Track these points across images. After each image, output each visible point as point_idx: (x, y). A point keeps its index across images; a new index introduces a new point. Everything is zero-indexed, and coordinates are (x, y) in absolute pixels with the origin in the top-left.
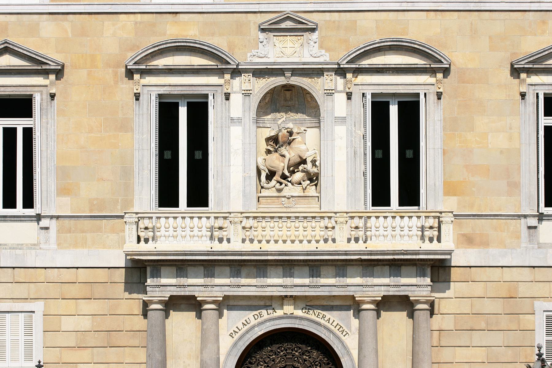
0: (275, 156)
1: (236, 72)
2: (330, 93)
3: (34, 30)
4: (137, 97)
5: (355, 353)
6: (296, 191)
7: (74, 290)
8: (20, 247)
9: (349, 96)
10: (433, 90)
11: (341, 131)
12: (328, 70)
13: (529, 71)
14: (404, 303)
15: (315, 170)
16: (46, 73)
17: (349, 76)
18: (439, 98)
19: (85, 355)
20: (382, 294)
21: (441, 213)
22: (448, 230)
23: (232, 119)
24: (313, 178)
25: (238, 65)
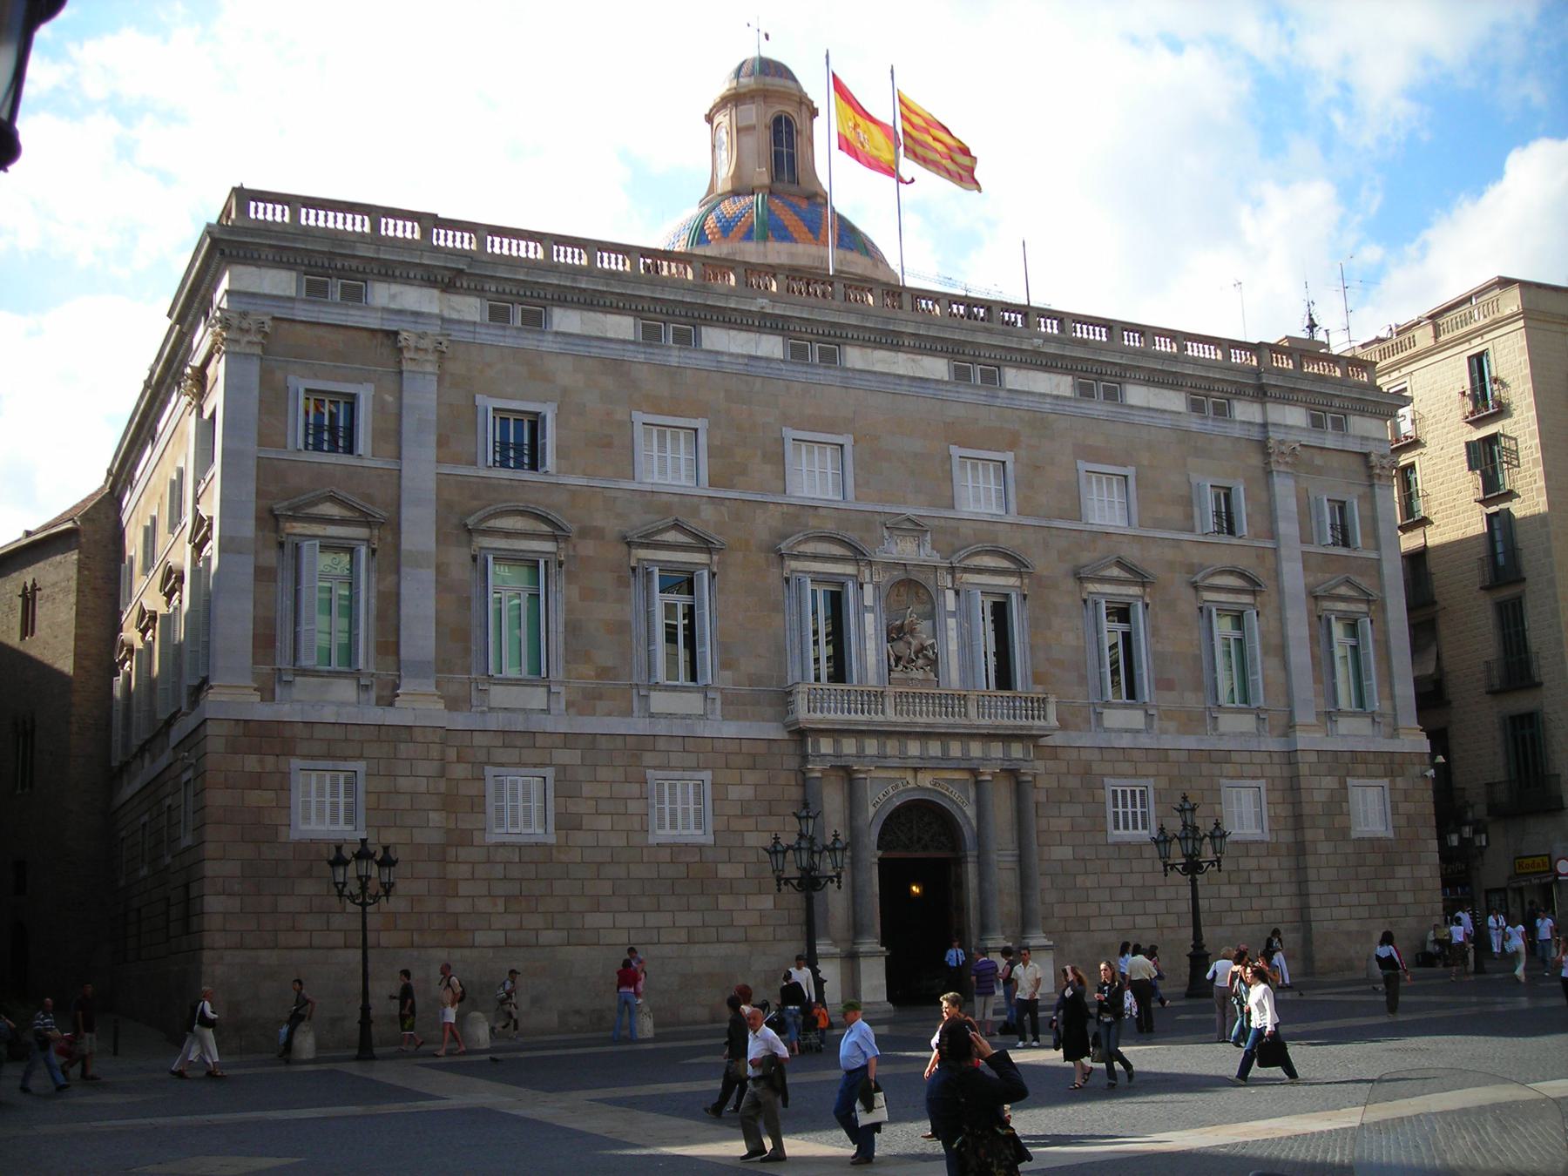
0: (901, 644)
1: (870, 563)
2: (941, 591)
3: (695, 511)
5: (974, 823)
6: (919, 675)
8: (688, 716)
9: (957, 593)
14: (1013, 774)
22: (1052, 710)
24: (933, 663)
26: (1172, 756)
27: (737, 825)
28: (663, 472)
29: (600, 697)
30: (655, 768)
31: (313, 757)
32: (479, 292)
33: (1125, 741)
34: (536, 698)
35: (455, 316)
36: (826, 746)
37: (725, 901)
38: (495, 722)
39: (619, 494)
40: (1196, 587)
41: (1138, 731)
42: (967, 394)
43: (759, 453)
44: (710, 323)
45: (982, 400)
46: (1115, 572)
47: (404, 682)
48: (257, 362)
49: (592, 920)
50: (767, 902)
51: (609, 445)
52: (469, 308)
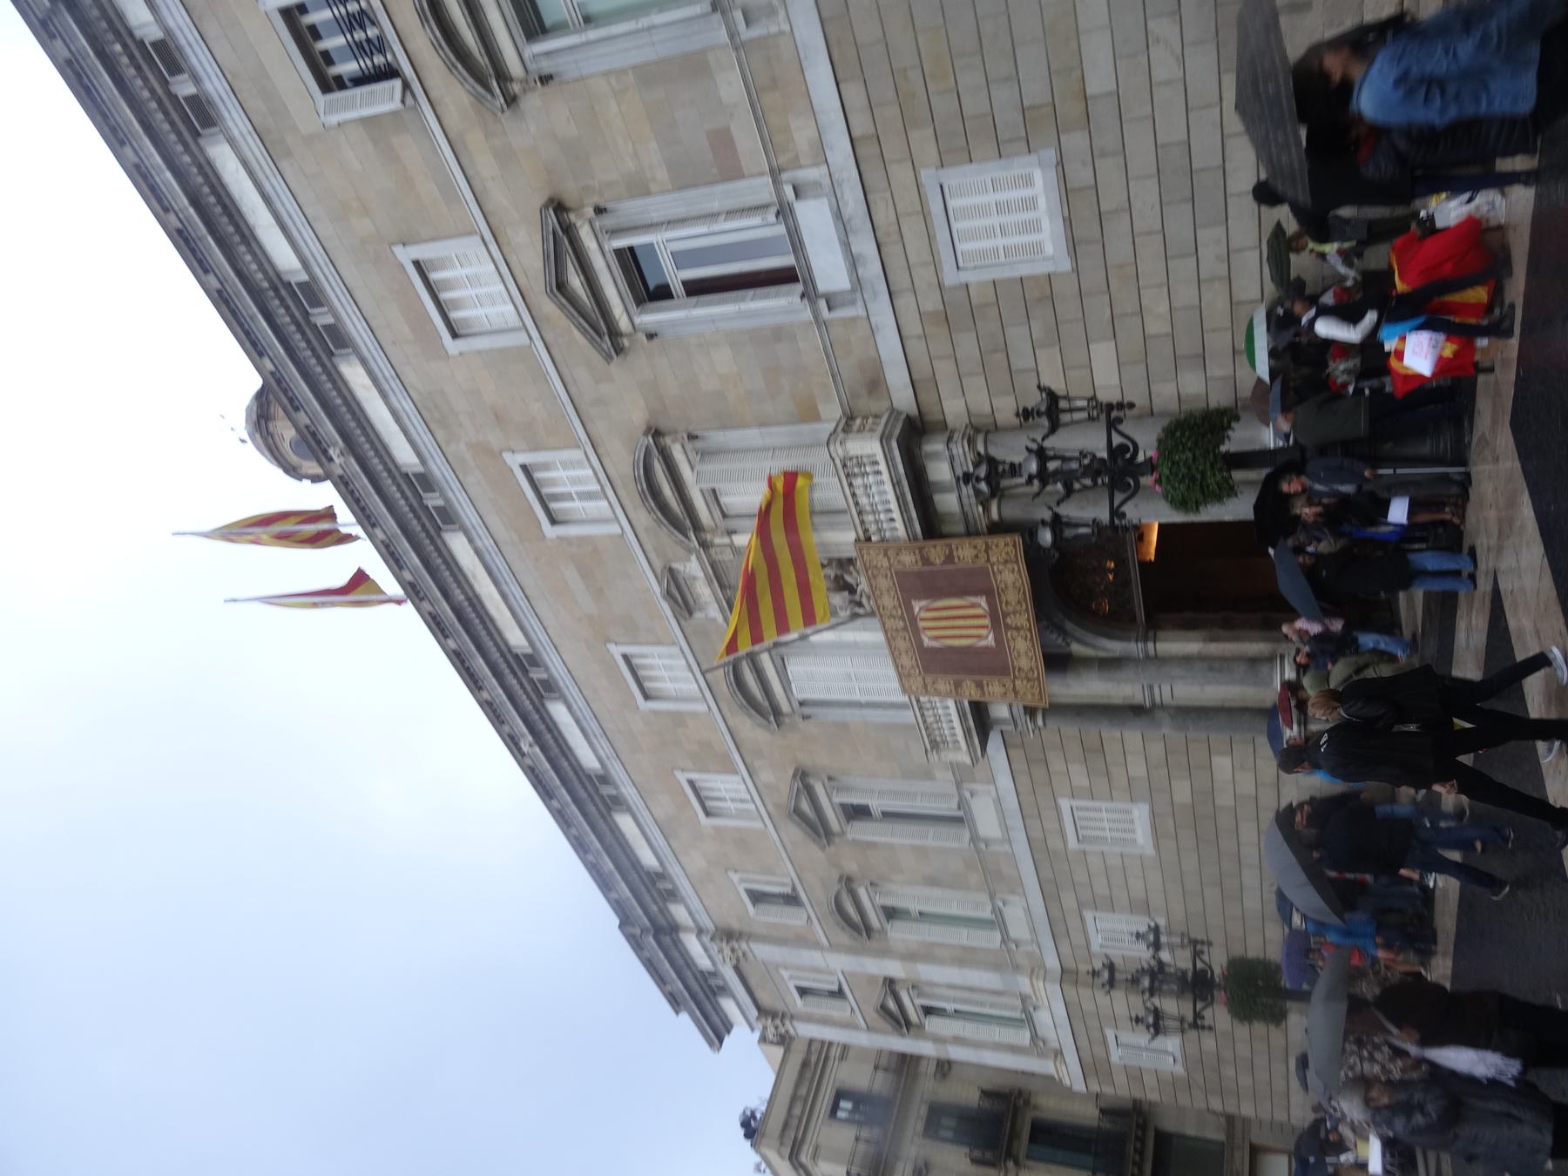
4: (805, 717)
9: (730, 533)
12: (709, 557)
13: (614, 333)
16: (809, 791)
17: (709, 537)
26: (861, 125)
30: (1065, 842)
32: (664, 912)
33: (865, 246)
34: (1015, 915)
37: (1225, 799)
39: (785, 840)
40: (511, 100)
41: (838, 215)
44: (577, 767)
45: (462, 497)
46: (575, 282)
48: (796, 1023)
50: (1222, 764)
52: (679, 912)
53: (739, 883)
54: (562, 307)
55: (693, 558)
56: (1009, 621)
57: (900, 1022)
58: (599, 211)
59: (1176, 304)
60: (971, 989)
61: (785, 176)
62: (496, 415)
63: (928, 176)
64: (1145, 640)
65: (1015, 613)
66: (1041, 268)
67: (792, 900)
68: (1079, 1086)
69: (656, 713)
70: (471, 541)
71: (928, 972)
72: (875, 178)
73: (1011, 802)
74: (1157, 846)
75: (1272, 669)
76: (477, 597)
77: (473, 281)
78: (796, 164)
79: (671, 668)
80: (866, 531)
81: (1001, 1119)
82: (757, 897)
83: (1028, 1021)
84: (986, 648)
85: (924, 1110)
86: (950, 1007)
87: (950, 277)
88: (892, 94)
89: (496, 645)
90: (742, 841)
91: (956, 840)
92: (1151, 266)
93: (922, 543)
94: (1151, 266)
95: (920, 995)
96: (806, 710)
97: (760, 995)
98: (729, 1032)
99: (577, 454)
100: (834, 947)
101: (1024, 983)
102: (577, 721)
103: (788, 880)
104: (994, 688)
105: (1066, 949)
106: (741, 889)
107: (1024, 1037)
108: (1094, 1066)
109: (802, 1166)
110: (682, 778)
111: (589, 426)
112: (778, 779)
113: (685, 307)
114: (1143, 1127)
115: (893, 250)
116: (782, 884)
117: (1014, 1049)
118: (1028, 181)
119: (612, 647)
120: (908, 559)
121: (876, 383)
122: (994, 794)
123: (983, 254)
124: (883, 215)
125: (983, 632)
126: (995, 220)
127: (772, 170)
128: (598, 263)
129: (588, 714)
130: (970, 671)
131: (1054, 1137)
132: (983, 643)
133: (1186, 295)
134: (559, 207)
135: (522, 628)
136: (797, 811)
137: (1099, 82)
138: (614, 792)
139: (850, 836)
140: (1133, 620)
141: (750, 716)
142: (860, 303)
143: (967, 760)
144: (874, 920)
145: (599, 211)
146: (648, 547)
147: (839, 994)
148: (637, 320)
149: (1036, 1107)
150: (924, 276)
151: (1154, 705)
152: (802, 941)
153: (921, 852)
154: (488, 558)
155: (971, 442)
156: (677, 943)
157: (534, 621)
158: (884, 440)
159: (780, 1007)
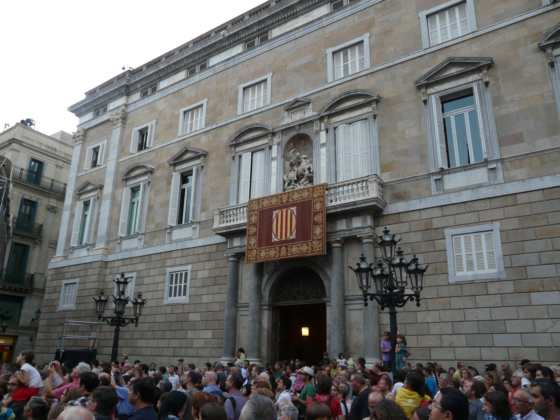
1: (274, 134)
2: (318, 133)
3: (198, 141)
7: (203, 257)
8: (185, 240)
9: (327, 132)
10: (370, 115)
11: (323, 150)
12: (316, 120)
13: (427, 86)
15: (311, 175)
16: (198, 157)
17: (326, 120)
18: (375, 118)
19: (205, 290)
20: (342, 236)
21: (368, 176)
23: (272, 158)
24: (311, 179)
25: (273, 130)
26: (521, 199)
27: (200, 291)
28: (191, 128)
29: (155, 237)
30: (170, 266)
31: (68, 279)
32: (136, 90)
33: (466, 196)
34: (134, 243)
35: (132, 102)
36: (237, 242)
37: (190, 334)
38: (120, 256)
41: (480, 186)
42: (339, 15)
43: (228, 101)
44: (210, 55)
45: (348, 13)
46: (453, 71)
47: (97, 245)
49: (141, 343)
51: (172, 127)
52: (136, 96)
53: (150, 124)
54: (442, 63)
55: (315, 113)
56: (283, 248)
57: (80, 192)
58: (487, 84)
59: (431, 325)
60: (97, 222)
61: (500, 165)
62: (388, 31)
63: (497, 225)
64: (269, 305)
65: (287, 251)
66: (450, 270)
67: (142, 146)
68: (50, 266)
69: (237, 93)
70: (326, 16)
71: (106, 205)
72: (496, 203)
73: (190, 244)
74: (168, 305)
75: (255, 357)
76: (298, 17)
77: (454, 27)
78: (505, 169)
79: (259, 98)
80: (331, 188)
81: (29, 232)
82: (143, 133)
83: (81, 246)
84: (271, 238)
85: (34, 199)
86: (89, 213)
87: (448, 232)
88: (536, 212)
89: (273, 23)
90: (172, 127)
91: (172, 219)
92: (448, 315)
93: (325, 212)
94: (448, 315)
95: (94, 200)
96: (237, 158)
97: (94, 131)
98: (76, 115)
99: (367, 65)
100: (118, 164)
101: (101, 245)
102: (234, 57)
103: (152, 145)
104: (253, 241)
105: (117, 264)
106: (149, 124)
107: (74, 244)
108: (59, 272)
109: (10, 144)
110: (204, 102)
111: (382, 72)
112: (203, 144)
113: (438, 117)
114: (26, 292)
115: (462, 209)
116: (150, 143)
117: (68, 239)
118: (491, 266)
119: (271, 74)
120: (318, 206)
121: (399, 197)
122: (194, 237)
123: (459, 246)
124: (479, 206)
125: (279, 237)
126: (474, 252)
127: (503, 159)
128: (462, 81)
129: (237, 62)
130: (260, 230)
131: (21, 254)
132: (273, 237)
133: (435, 329)
134: (490, 66)
135: (278, 37)
136: (187, 151)
137: (536, 298)
138: (197, 71)
139: (174, 174)
140: (277, 301)
141: (236, 133)
142: (437, 193)
143: (214, 227)
144: (132, 182)
145: (487, 84)
146: (320, 94)
147: (94, 164)
148: (433, 96)
149: (34, 247)
150: (450, 221)
151: (237, 307)
152: (122, 151)
153: (167, 203)
154: (317, 23)
155: (370, 237)
156: (121, 95)
157: (284, 41)
158: (376, 199)
159: (88, 139)
